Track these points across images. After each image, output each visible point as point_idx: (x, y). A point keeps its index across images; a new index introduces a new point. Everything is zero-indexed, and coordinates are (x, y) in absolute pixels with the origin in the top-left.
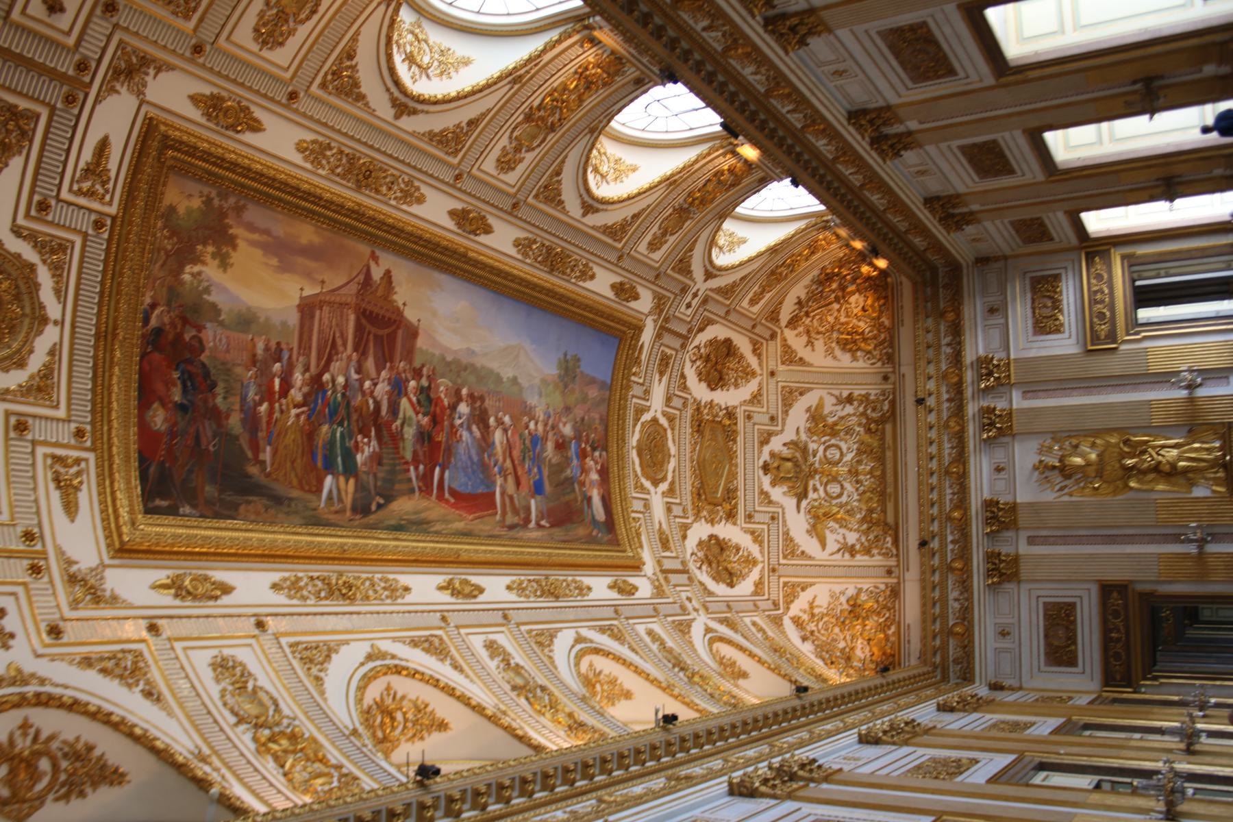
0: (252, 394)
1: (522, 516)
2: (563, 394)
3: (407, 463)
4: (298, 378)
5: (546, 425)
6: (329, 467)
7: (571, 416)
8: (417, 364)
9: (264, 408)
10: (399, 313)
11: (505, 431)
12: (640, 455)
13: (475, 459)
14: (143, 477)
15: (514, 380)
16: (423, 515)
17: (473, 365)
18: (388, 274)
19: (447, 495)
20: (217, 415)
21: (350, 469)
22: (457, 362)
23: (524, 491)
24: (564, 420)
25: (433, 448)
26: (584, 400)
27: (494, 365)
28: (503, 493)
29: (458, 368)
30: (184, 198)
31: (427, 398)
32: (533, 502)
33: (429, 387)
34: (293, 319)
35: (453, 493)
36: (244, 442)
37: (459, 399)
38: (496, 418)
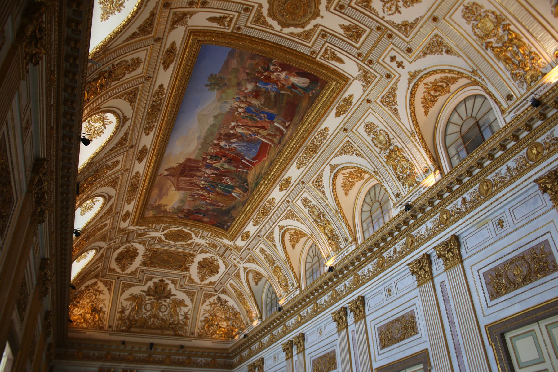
0: (204, 203)
1: (278, 133)
2: (229, 87)
3: (237, 170)
4: (200, 192)
5: (243, 102)
6: (230, 192)
7: (243, 82)
8: (201, 159)
9: (208, 201)
10: (181, 164)
11: (238, 126)
12: (289, 26)
13: (245, 144)
14: (218, 227)
15: (216, 117)
16: (257, 174)
17: (205, 137)
18: (166, 170)
19: (254, 162)
20: (207, 210)
21: (233, 188)
22: (202, 144)
23: (268, 126)
24: (244, 89)
25: (235, 159)
26: (236, 71)
27: (206, 127)
28: (265, 138)
29: (205, 143)
30: (150, 214)
31: (215, 157)
32: (275, 124)
33: (211, 155)
34: (182, 192)
35: (254, 159)
36: (216, 208)
37: (218, 144)
38: (232, 129)
